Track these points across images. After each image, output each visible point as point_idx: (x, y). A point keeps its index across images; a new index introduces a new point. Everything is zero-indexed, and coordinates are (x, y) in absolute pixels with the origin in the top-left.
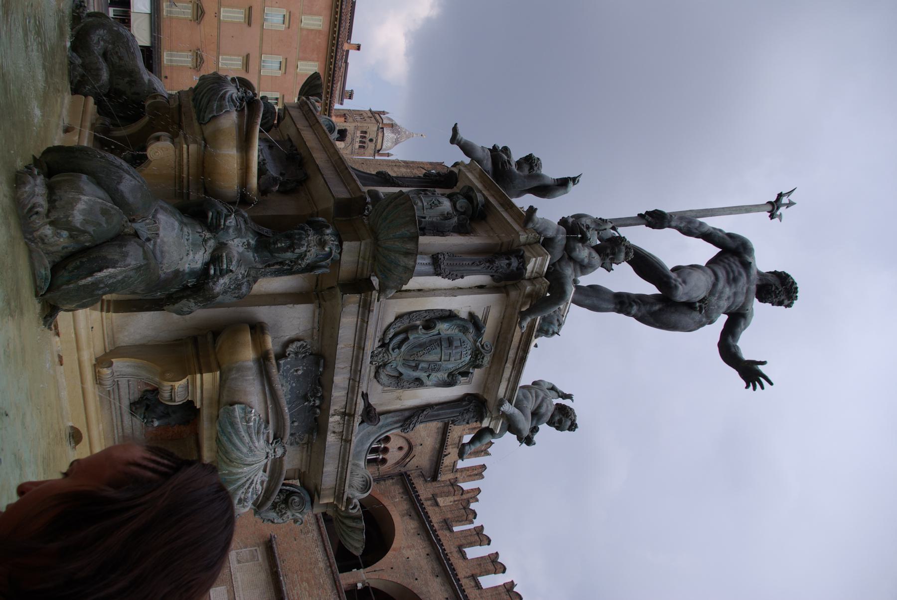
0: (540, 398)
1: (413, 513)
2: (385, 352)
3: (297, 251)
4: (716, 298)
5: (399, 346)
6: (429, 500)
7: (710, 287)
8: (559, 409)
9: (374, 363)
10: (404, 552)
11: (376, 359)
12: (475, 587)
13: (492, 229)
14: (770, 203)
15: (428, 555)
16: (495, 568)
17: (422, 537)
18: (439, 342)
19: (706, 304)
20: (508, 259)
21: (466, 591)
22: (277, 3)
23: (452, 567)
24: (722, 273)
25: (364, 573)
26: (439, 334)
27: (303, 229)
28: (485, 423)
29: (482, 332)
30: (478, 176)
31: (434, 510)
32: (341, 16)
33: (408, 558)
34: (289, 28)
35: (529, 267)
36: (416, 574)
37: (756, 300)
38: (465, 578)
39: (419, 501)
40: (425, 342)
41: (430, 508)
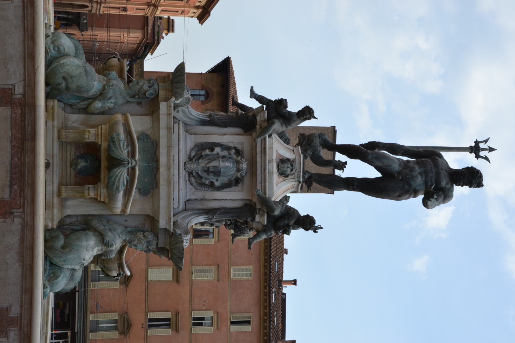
2: (192, 163)
3: (140, 84)
4: (408, 171)
5: (198, 159)
9: (187, 170)
11: (187, 166)
18: (217, 157)
19: (402, 174)
22: (204, 305)
26: (218, 154)
28: (257, 218)
29: (241, 154)
32: (270, 310)
34: (218, 329)
35: (258, 118)
40: (211, 158)
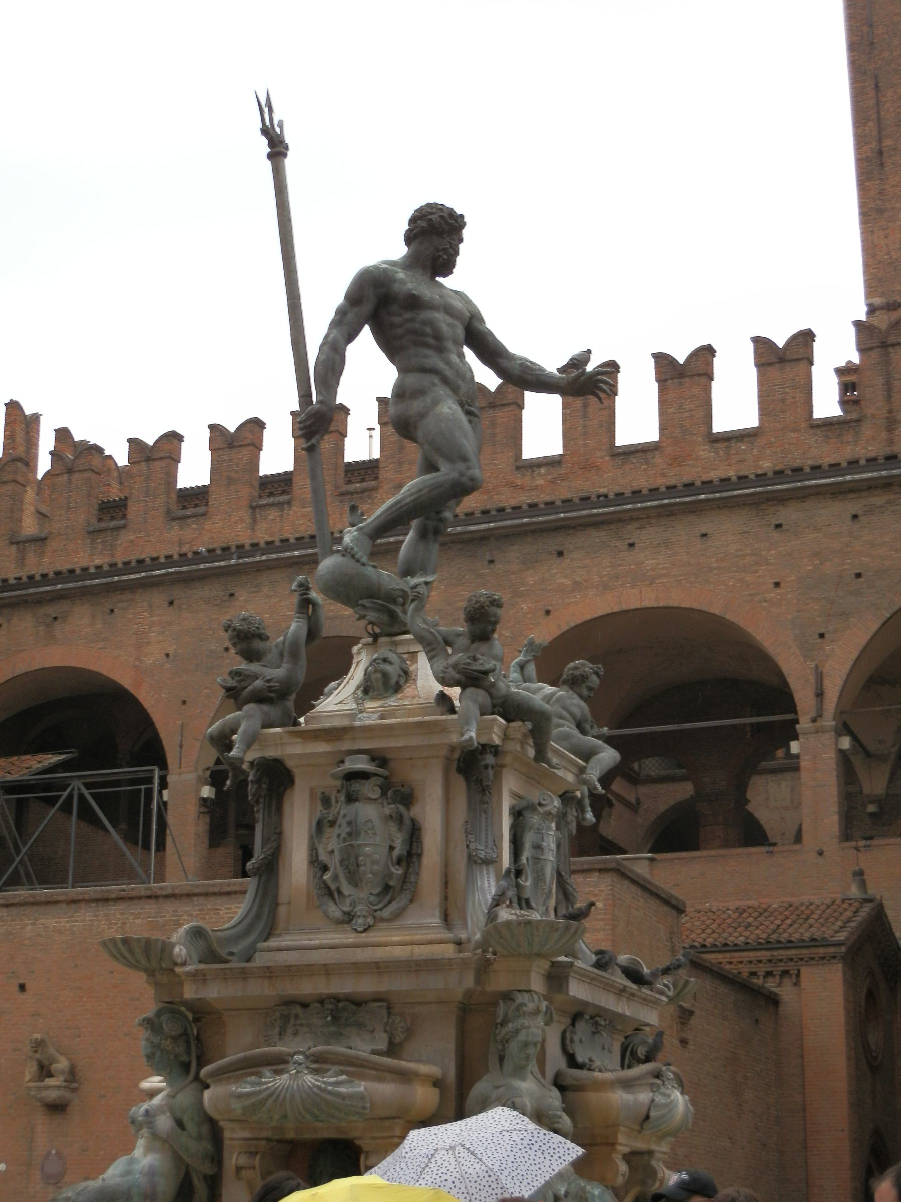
0: (564, 713)
1: (51, 610)
4: (463, 385)
6: (23, 559)
7: (449, 392)
8: (573, 683)
10: (149, 661)
12: (282, 510)
13: (411, 759)
14: (270, 156)
15: (171, 603)
16: (249, 445)
17: (120, 604)
20: (486, 767)
21: (286, 536)
23: (219, 552)
24: (426, 356)
25: (180, 774)
27: (517, 1031)
30: (300, 740)
31: (54, 551)
33: (167, 655)
36: (213, 647)
37: (448, 282)
38: (253, 530)
39: (20, 584)
41: (46, 560)
